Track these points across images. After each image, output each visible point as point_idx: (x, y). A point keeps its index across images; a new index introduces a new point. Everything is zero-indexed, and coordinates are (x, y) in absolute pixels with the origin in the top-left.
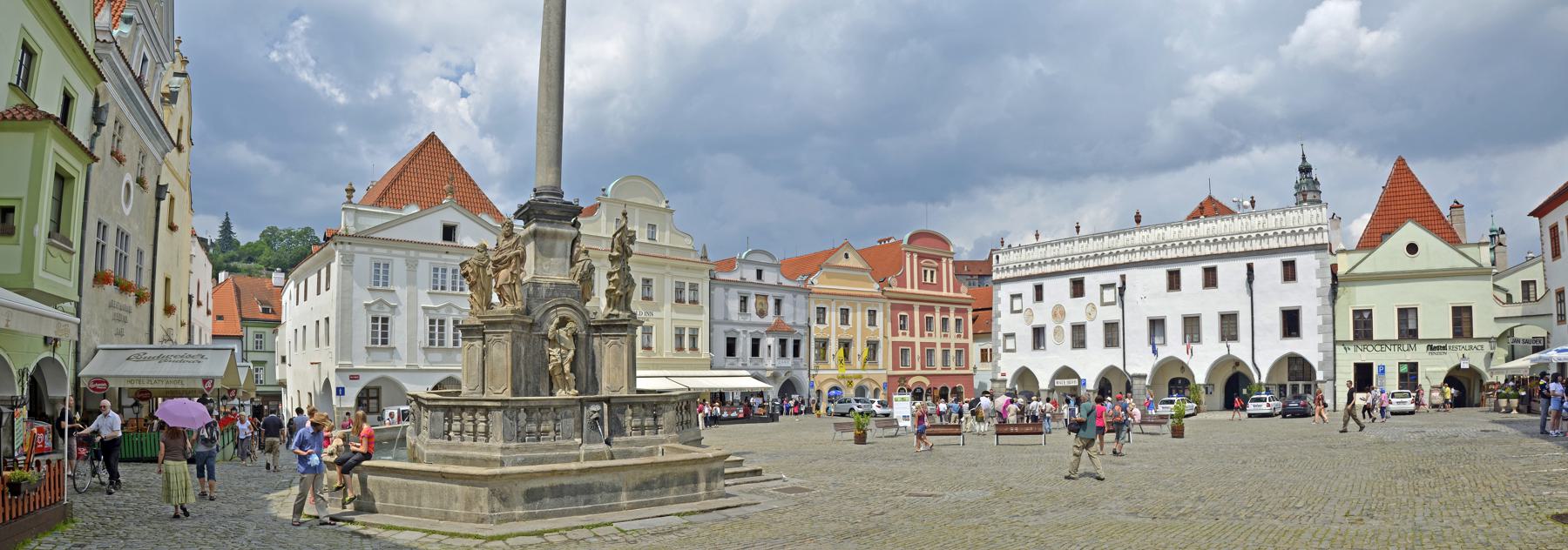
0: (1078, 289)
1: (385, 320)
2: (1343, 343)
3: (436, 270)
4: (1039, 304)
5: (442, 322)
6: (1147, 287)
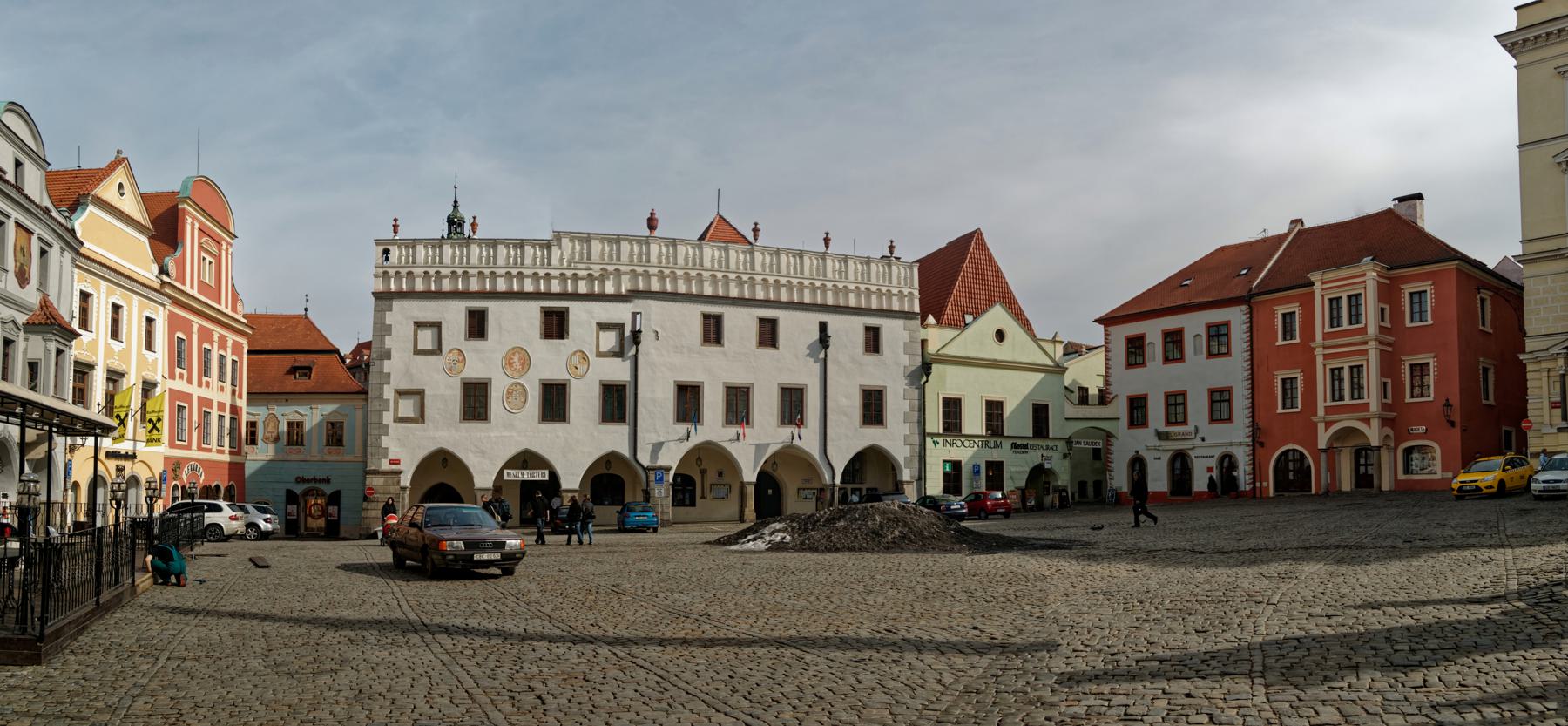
0: (556, 325)
2: (932, 435)
4: (477, 344)
6: (671, 333)
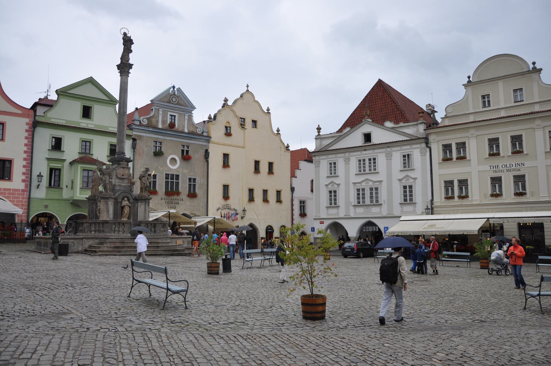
1: (335, 192)
3: (360, 161)
5: (363, 190)
